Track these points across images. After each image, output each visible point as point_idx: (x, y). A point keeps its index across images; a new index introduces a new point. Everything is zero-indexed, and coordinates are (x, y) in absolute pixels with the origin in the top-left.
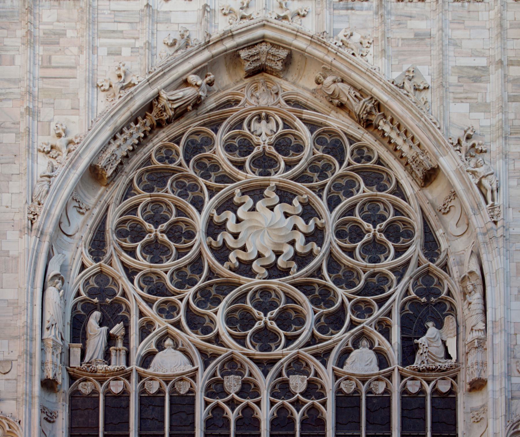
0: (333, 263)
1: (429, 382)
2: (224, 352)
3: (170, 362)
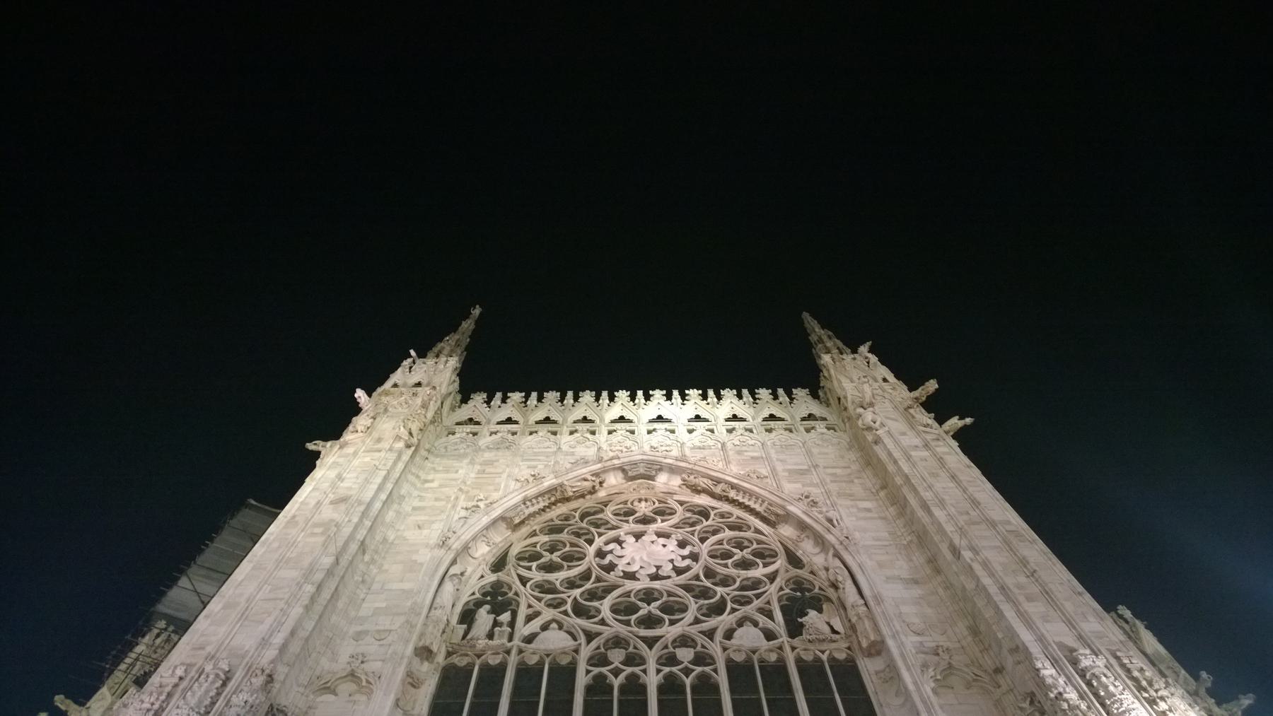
0: (709, 573)
1: (823, 652)
2: (607, 632)
3: (555, 641)
